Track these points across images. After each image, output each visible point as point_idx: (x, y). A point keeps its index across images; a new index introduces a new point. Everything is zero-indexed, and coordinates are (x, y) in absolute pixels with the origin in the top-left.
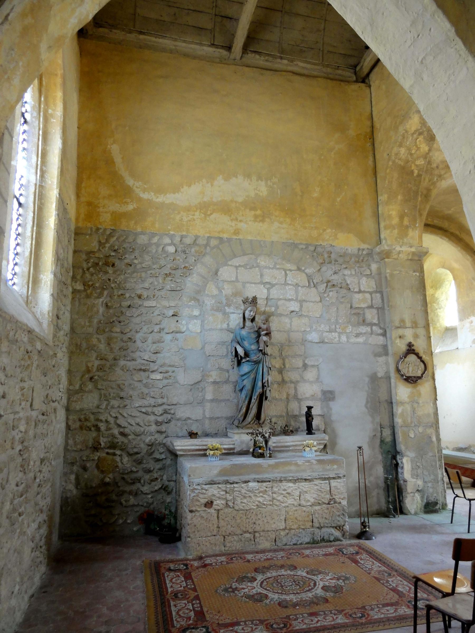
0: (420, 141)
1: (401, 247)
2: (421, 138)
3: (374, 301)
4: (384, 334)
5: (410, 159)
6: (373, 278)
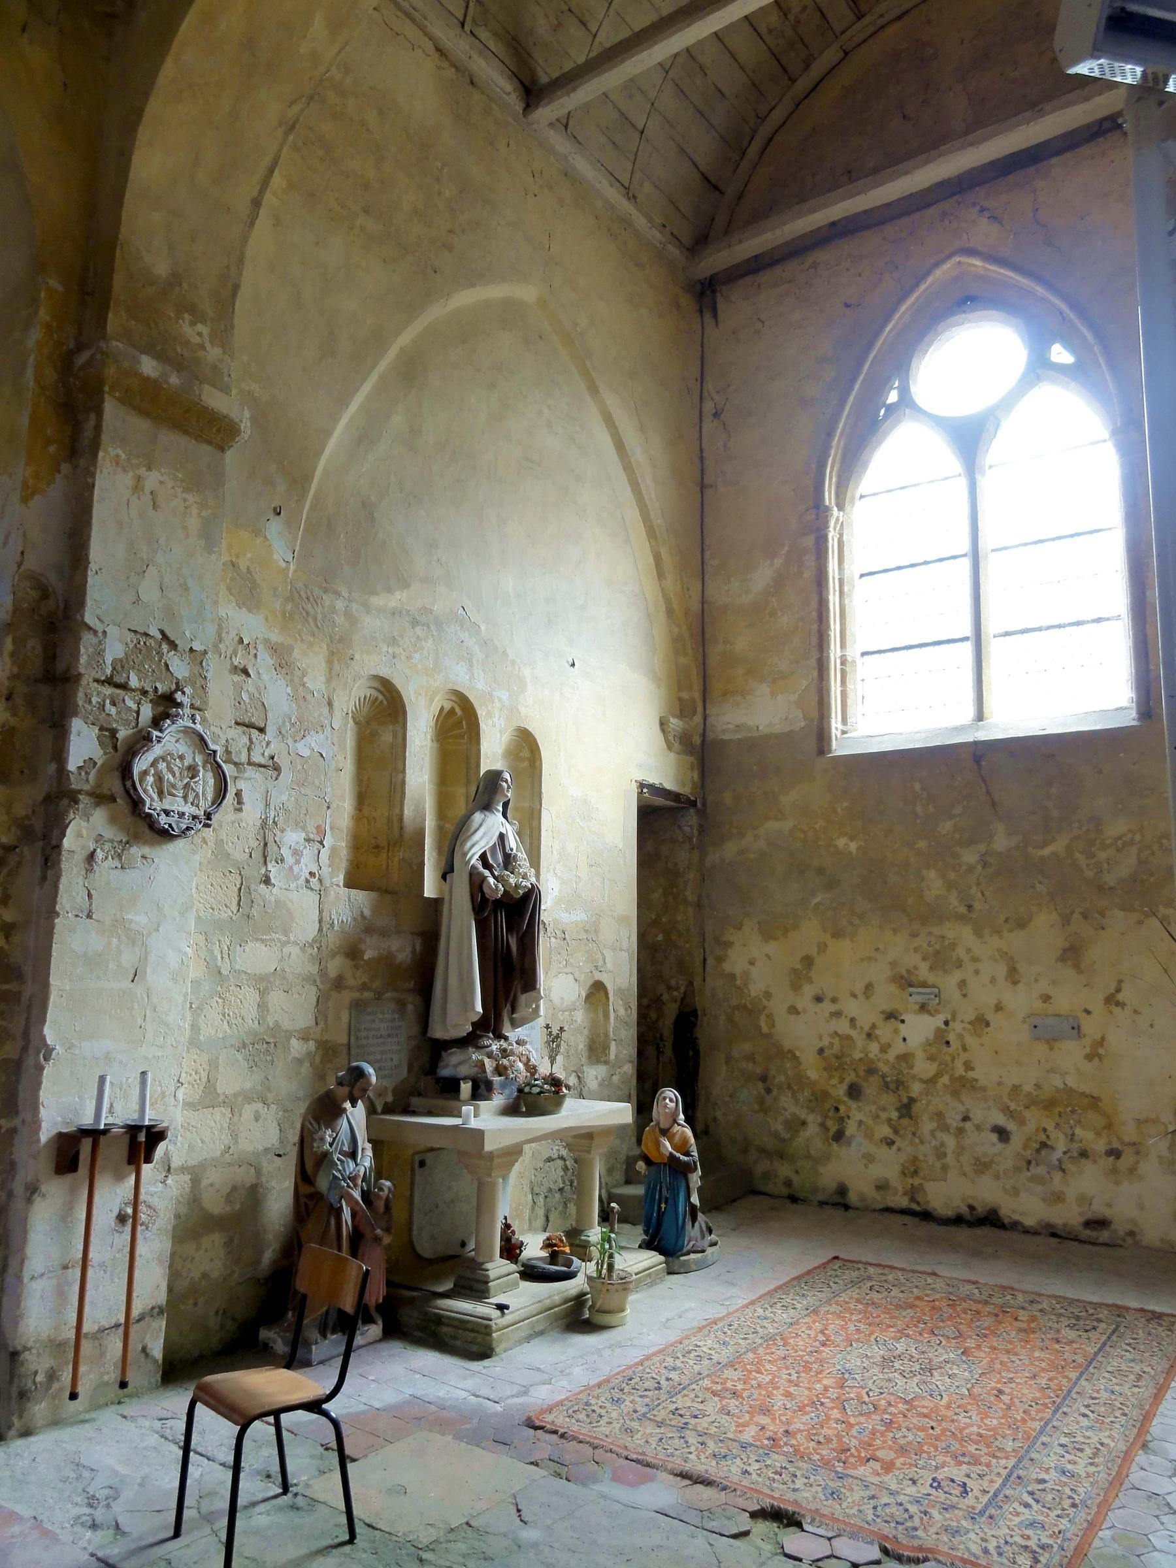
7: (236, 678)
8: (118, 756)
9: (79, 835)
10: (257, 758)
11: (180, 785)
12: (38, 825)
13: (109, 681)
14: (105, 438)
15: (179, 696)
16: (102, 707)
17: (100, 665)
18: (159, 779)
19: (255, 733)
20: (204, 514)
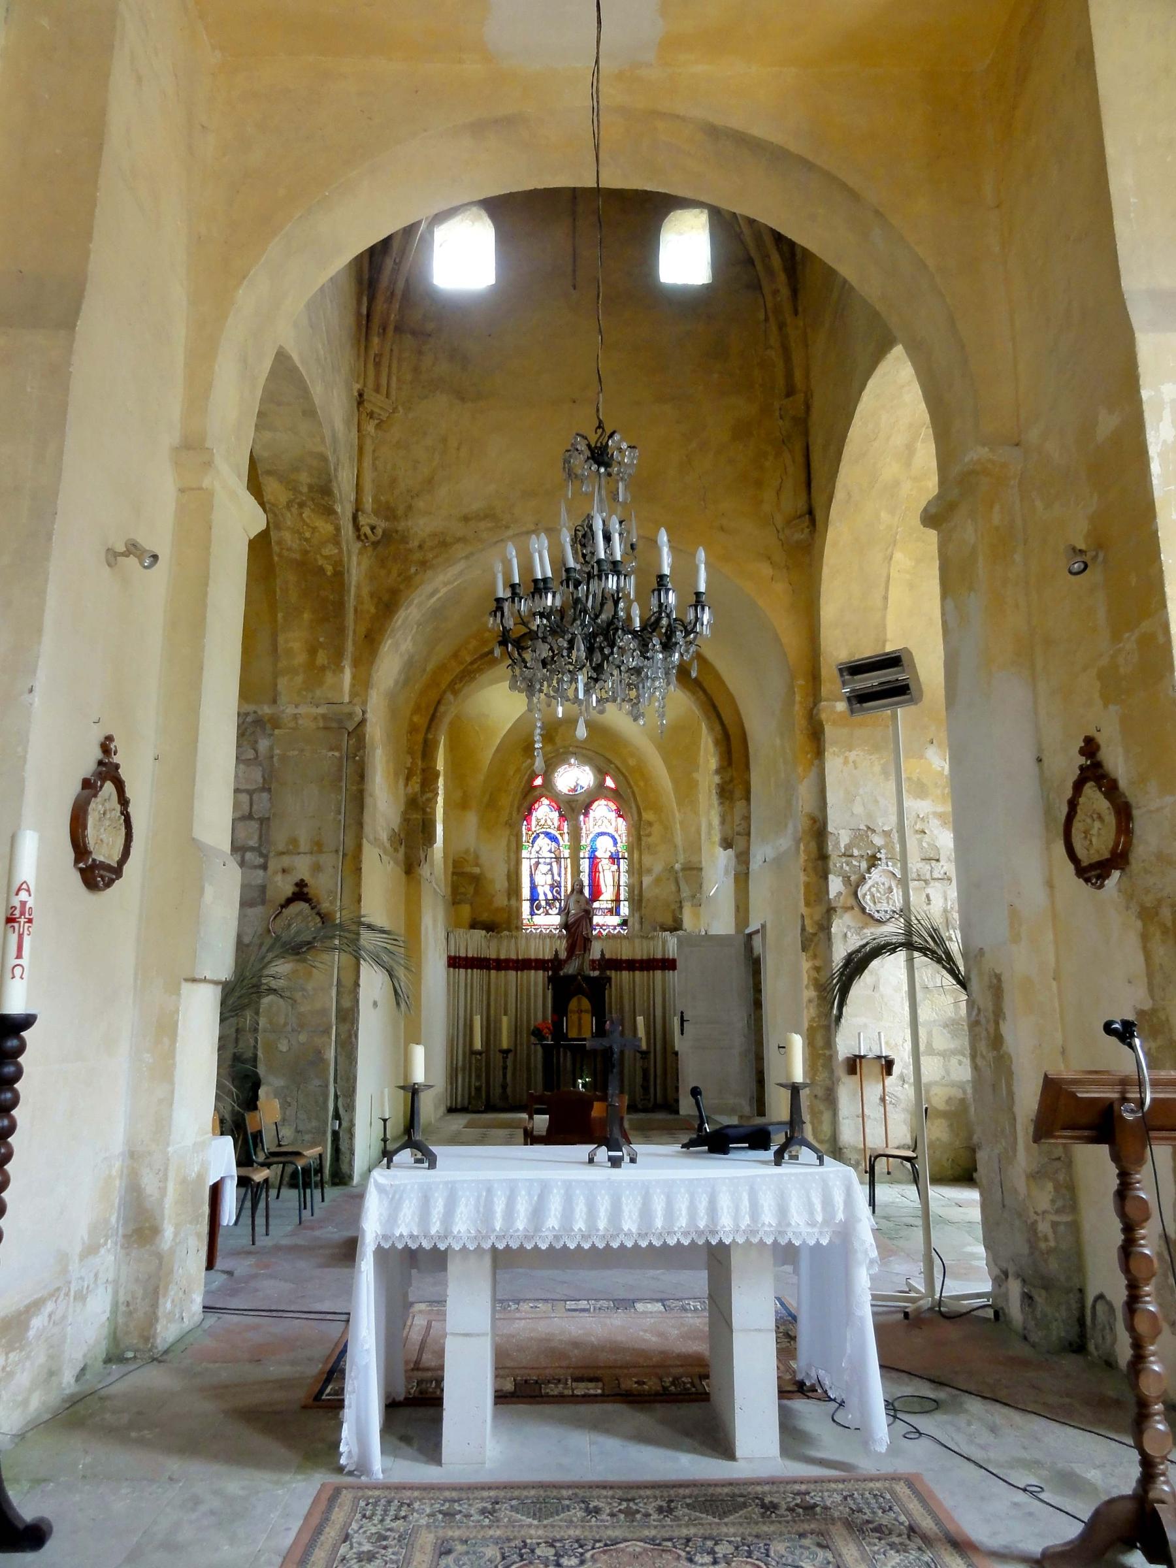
0: (309, 517)
1: (296, 706)
2: (306, 513)
3: (255, 807)
4: (264, 867)
5: (308, 548)
6: (261, 765)
7: (918, 836)
8: (853, 889)
9: (839, 926)
10: (936, 875)
11: (884, 897)
12: (825, 923)
13: (844, 855)
14: (827, 745)
15: (878, 855)
16: (842, 867)
17: (839, 849)
18: (873, 896)
19: (933, 863)
20: (882, 762)
